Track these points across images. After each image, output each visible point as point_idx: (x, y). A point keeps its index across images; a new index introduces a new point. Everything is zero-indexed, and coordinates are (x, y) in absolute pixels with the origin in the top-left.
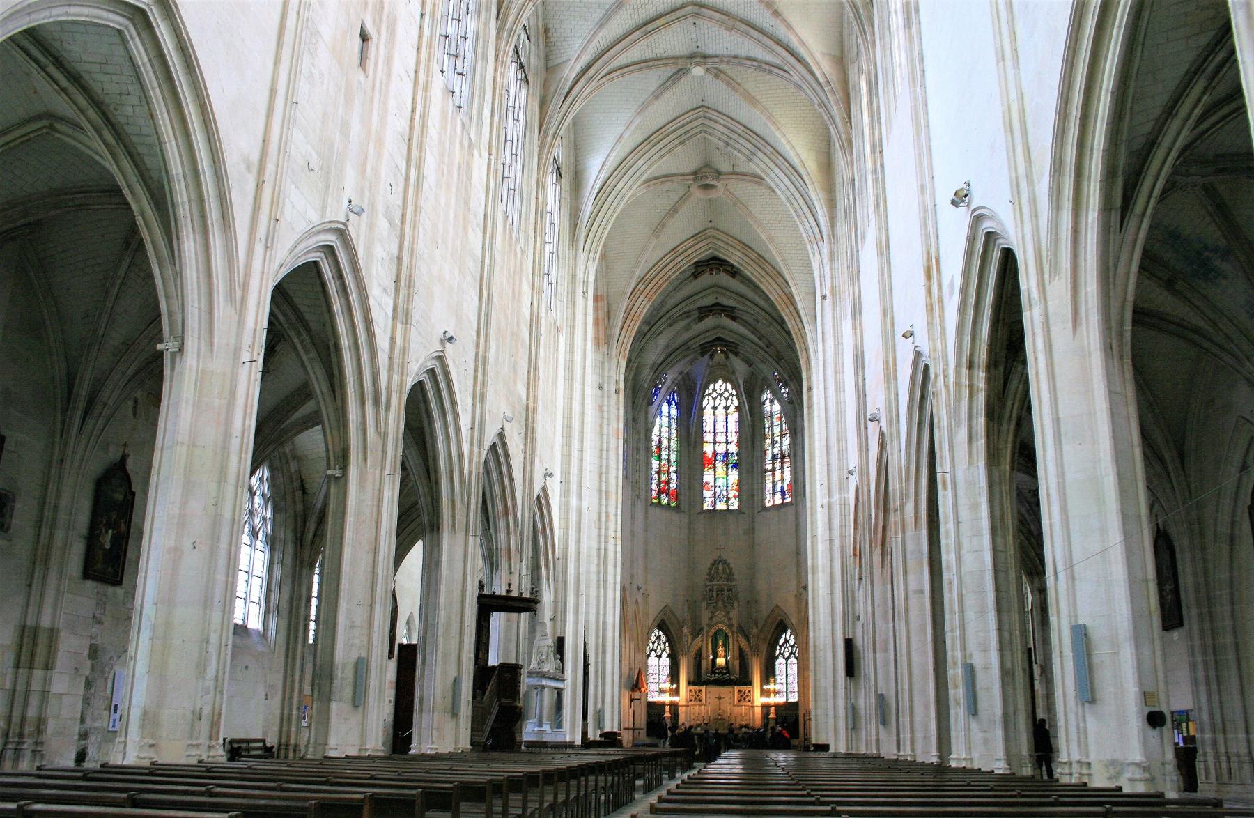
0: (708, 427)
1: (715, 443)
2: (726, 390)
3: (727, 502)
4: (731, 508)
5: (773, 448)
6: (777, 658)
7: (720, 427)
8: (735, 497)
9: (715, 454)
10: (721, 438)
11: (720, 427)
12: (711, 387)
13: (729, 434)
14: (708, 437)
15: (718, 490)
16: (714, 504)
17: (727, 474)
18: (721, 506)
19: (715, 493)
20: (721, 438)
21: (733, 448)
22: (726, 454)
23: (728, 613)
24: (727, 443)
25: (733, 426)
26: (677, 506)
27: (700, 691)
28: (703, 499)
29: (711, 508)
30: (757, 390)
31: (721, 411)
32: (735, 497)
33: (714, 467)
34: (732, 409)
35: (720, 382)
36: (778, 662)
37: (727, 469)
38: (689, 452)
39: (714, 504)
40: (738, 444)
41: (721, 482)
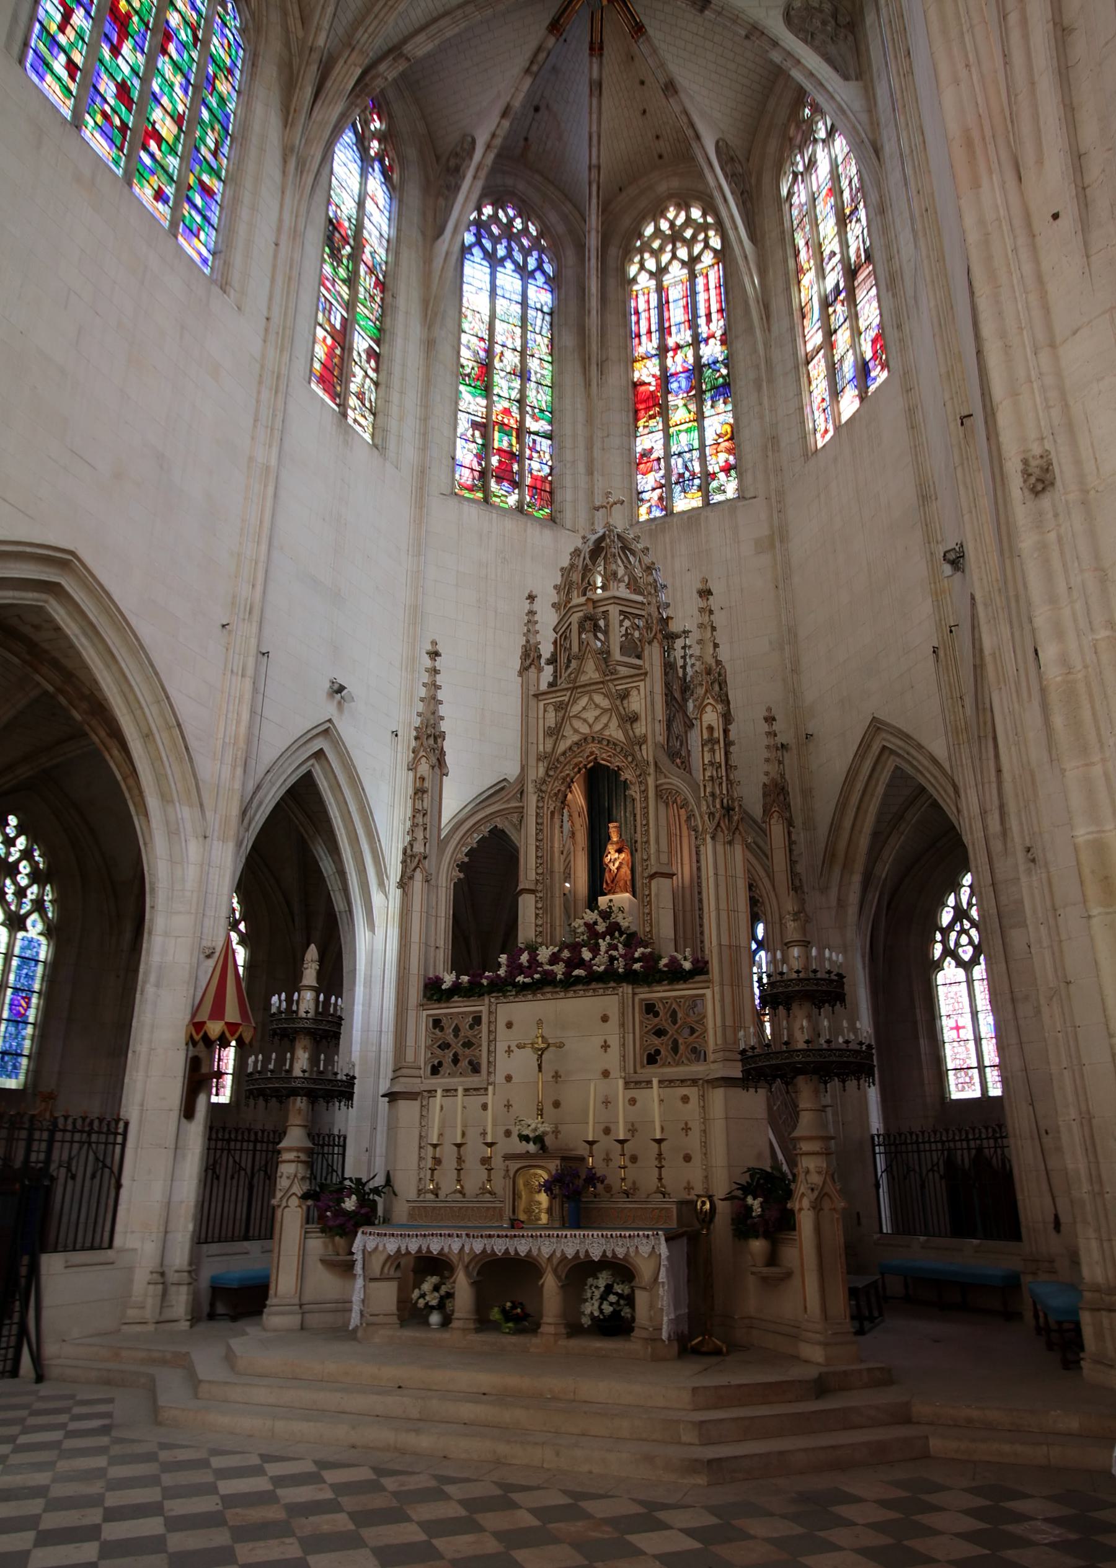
0: (646, 321)
1: (663, 350)
2: (689, 221)
3: (704, 489)
4: (717, 498)
5: (821, 274)
6: (938, 966)
7: (677, 314)
8: (727, 469)
9: (665, 378)
10: (680, 336)
11: (677, 314)
12: (649, 230)
13: (702, 321)
14: (648, 346)
15: (677, 464)
16: (666, 502)
17: (700, 417)
18: (685, 502)
19: (668, 475)
20: (680, 336)
21: (712, 351)
22: (697, 369)
23: (624, 696)
24: (697, 341)
25: (709, 297)
26: (552, 519)
27: (477, 1020)
28: (638, 497)
29: (657, 513)
30: (767, 179)
31: (677, 272)
32: (727, 469)
33: (664, 412)
34: (708, 258)
35: (671, 214)
36: (941, 978)
37: (700, 403)
38: (588, 384)
39: (666, 502)
40: (723, 342)
41: (684, 440)
